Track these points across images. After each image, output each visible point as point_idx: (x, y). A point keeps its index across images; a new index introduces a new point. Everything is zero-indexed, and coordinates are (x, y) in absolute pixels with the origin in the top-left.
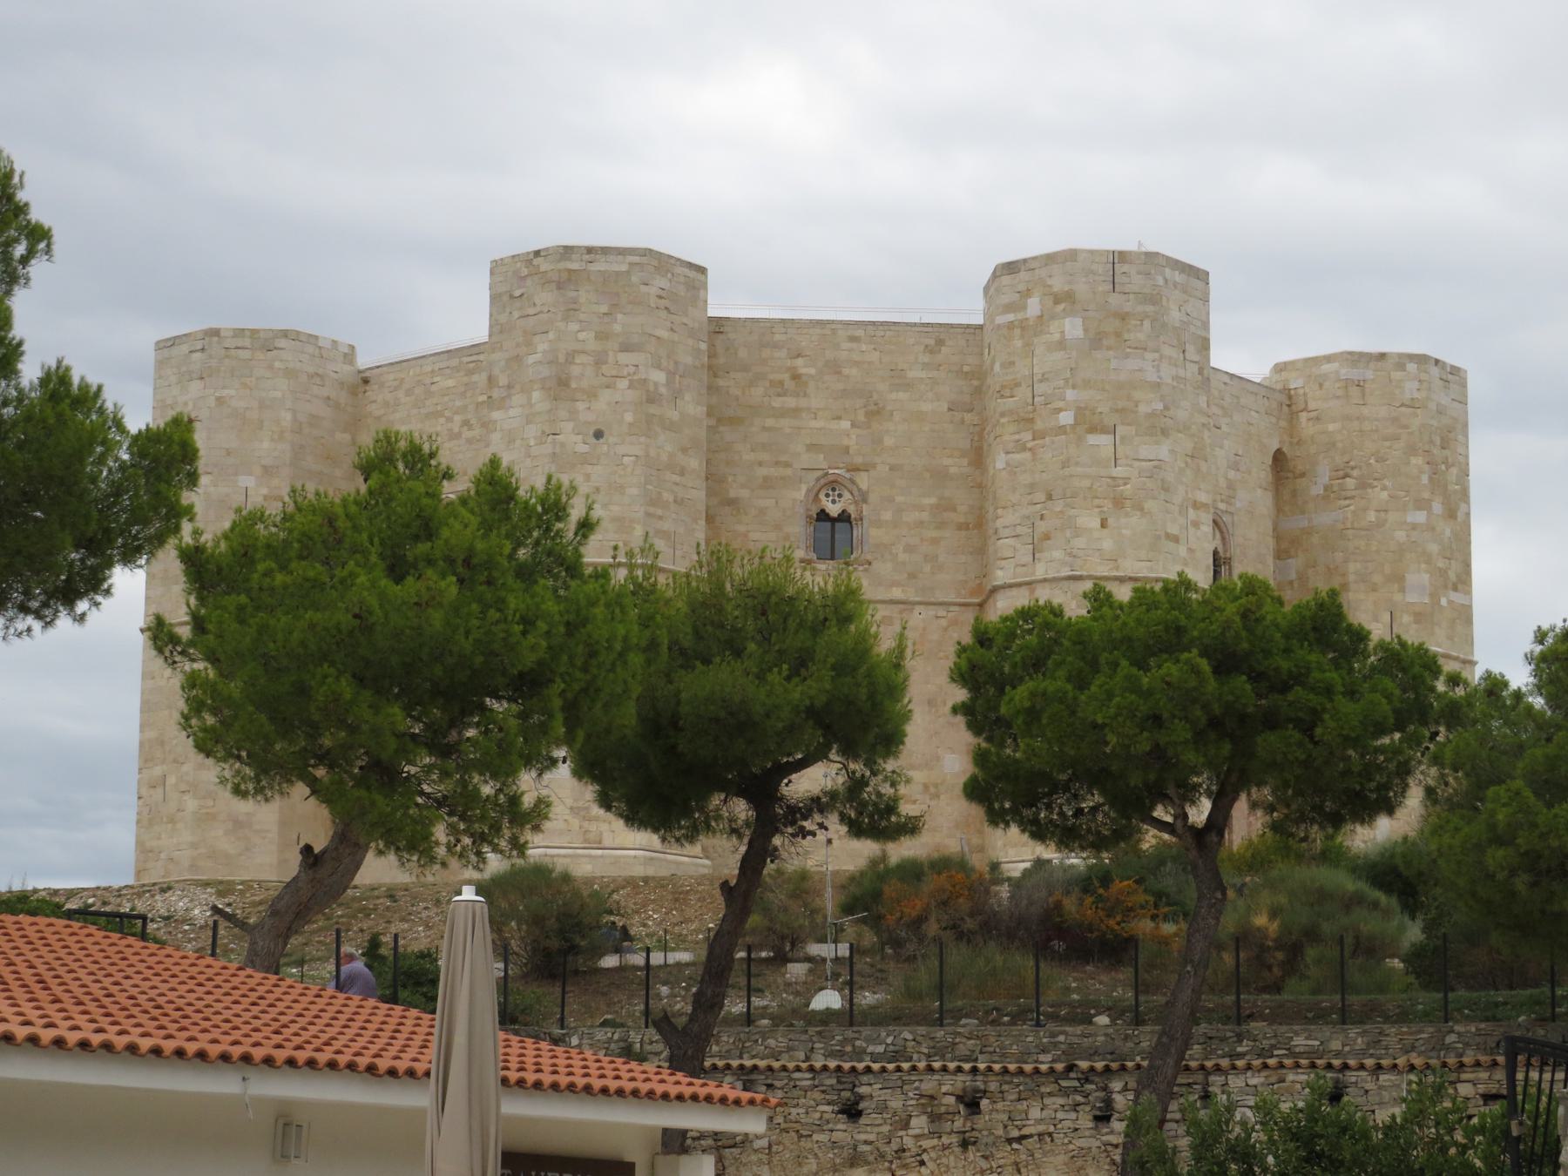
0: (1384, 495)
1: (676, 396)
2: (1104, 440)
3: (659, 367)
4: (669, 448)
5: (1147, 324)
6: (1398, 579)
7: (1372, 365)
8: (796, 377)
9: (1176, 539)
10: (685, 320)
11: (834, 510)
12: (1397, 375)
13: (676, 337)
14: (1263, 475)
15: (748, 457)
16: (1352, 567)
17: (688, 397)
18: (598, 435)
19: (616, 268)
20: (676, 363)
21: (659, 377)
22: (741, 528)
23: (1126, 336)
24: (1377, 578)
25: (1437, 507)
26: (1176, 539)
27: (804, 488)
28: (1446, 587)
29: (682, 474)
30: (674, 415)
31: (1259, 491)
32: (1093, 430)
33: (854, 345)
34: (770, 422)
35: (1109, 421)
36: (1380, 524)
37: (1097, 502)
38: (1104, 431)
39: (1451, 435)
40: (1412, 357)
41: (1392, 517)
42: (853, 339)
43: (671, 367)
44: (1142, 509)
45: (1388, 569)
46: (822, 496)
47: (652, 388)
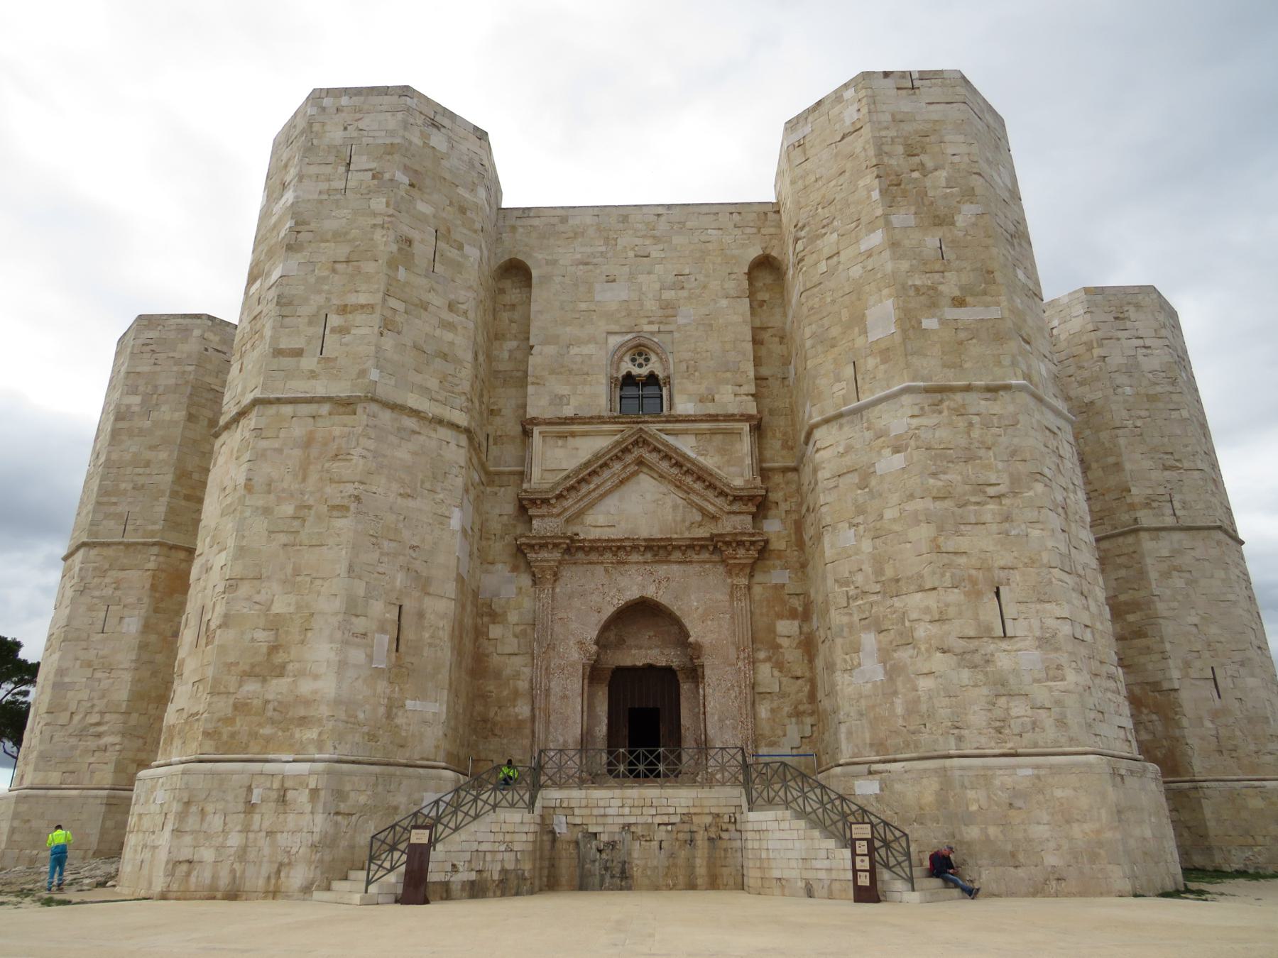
0: (835, 235)
4: (134, 449)
6: (859, 321)
7: (810, 119)
9: (298, 353)
10: (171, 355)
13: (158, 368)
14: (730, 285)
16: (807, 332)
17: (164, 408)
20: (156, 387)
21: (136, 400)
24: (835, 331)
25: (903, 217)
39: (933, 138)
40: (846, 86)
45: (845, 315)
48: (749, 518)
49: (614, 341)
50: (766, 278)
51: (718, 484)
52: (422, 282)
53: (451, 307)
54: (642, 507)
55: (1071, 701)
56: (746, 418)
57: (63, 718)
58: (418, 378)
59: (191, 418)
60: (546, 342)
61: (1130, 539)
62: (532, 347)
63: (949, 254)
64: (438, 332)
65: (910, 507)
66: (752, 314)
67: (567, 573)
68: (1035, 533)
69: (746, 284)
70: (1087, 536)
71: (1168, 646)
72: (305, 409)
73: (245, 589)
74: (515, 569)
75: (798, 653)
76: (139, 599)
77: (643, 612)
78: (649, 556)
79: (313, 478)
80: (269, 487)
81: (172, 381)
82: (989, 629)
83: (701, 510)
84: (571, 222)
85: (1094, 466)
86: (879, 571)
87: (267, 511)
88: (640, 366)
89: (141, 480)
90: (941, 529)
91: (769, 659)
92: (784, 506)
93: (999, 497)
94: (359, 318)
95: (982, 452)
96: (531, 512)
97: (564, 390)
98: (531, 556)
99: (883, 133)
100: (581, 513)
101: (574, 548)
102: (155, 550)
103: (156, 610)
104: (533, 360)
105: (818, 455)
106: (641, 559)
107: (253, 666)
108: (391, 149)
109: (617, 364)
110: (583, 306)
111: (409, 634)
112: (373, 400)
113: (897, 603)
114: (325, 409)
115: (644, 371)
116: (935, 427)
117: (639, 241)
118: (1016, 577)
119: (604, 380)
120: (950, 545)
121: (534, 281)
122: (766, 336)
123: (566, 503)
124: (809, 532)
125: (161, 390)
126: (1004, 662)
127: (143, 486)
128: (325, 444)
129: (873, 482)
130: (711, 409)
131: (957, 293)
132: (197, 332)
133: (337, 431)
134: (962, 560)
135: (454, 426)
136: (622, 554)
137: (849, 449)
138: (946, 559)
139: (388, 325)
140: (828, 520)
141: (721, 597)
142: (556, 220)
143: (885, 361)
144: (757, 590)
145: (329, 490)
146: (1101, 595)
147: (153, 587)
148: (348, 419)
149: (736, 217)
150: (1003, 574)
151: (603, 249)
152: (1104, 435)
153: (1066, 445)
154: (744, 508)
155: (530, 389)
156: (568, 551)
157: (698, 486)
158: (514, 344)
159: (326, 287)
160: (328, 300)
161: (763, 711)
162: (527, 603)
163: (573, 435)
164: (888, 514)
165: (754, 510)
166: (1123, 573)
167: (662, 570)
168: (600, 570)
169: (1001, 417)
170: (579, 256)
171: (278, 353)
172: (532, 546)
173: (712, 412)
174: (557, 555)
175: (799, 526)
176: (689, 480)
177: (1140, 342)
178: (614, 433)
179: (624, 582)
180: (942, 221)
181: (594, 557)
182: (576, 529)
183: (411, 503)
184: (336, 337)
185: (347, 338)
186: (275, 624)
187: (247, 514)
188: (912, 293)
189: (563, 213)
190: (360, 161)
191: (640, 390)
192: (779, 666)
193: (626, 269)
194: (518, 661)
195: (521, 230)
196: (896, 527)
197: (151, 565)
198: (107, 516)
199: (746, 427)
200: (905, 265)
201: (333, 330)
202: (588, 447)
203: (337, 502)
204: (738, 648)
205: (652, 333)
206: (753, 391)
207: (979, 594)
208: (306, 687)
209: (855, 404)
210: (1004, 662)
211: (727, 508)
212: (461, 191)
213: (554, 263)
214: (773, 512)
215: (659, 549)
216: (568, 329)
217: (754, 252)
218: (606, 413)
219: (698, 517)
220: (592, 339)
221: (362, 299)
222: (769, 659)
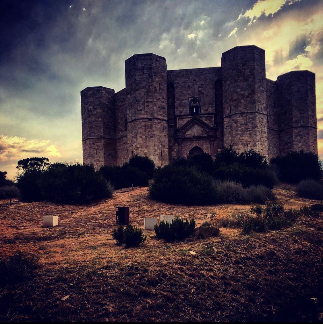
1: (95, 109)
2: (129, 96)
3: (91, 106)
4: (94, 118)
8: (124, 99)
9: (141, 110)
13: (95, 100)
18: (85, 119)
21: (92, 107)
28: (244, 97)
29: (97, 121)
30: (95, 113)
31: (210, 90)
34: (121, 108)
36: (228, 89)
41: (231, 86)
45: (230, 98)
47: (89, 110)
49: (190, 99)
53: (163, 98)
56: (213, 114)
58: (159, 113)
59: (104, 111)
60: (178, 100)
64: (162, 104)
65: (236, 133)
66: (215, 92)
68: (254, 136)
72: (144, 120)
73: (140, 149)
76: (102, 149)
77: (196, 148)
78: (197, 139)
79: (147, 132)
81: (98, 103)
83: (206, 131)
86: (232, 142)
87: (141, 137)
88: (195, 104)
89: (97, 125)
90: (240, 136)
92: (220, 129)
93: (250, 131)
94: (150, 104)
95: (248, 123)
97: (182, 110)
100: (186, 132)
102: (103, 139)
103: (105, 150)
104: (176, 104)
106: (195, 140)
110: (184, 92)
112: (154, 118)
114: (147, 120)
116: (241, 120)
117: (194, 77)
120: (241, 139)
125: (96, 105)
128: (148, 126)
129: (232, 128)
130: (207, 112)
131: (248, 95)
132: (100, 91)
134: (243, 141)
135: (165, 120)
138: (240, 141)
142: (178, 73)
143: (235, 107)
144: (215, 144)
145: (150, 133)
147: (104, 146)
148: (151, 122)
149: (213, 71)
150: (249, 143)
151: (187, 79)
153: (265, 120)
155: (176, 110)
158: (172, 100)
159: (144, 98)
160: (144, 100)
163: (184, 118)
164: (234, 133)
168: (189, 142)
169: (252, 117)
171: (138, 110)
173: (207, 113)
174: (182, 140)
178: (190, 118)
180: (247, 80)
182: (185, 135)
183: (161, 134)
187: (138, 137)
188: (240, 95)
193: (192, 83)
196: (235, 136)
198: (92, 133)
199: (214, 115)
200: (239, 90)
201: (146, 106)
202: (186, 120)
203: (151, 135)
207: (245, 146)
213: (178, 83)
215: (198, 138)
217: (216, 79)
219: (205, 132)
220: (186, 99)
221: (150, 100)
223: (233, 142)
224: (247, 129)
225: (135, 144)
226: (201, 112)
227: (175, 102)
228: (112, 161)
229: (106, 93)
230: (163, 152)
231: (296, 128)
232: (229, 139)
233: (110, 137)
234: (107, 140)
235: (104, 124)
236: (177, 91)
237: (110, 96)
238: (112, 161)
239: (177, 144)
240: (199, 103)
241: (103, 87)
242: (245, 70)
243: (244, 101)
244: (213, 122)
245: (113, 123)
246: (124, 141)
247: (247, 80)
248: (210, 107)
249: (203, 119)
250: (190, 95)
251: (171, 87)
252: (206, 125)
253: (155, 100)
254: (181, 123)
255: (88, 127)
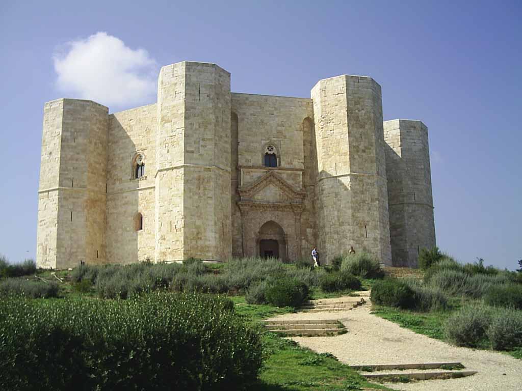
2: (168, 125)
3: (67, 131)
4: (71, 153)
5: (182, 84)
9: (193, 152)
10: (79, 116)
11: (140, 163)
12: (337, 84)
14: (298, 126)
15: (119, 152)
18: (50, 153)
19: (56, 106)
20: (75, 129)
21: (68, 134)
22: (116, 173)
23: (176, 90)
24: (331, 153)
26: (193, 152)
27: (131, 158)
28: (358, 151)
29: (77, 160)
30: (74, 144)
31: (296, 132)
32: (167, 122)
33: (144, 113)
34: (124, 141)
35: (170, 119)
37: (167, 145)
38: (169, 122)
39: (361, 100)
42: (144, 111)
43: (73, 130)
44: (179, 144)
45: (334, 150)
46: (137, 159)
48: (301, 200)
50: (307, 123)
51: (293, 189)
52: (221, 130)
53: (226, 135)
54: (270, 193)
55: (379, 252)
56: (301, 170)
57: (63, 250)
59: (90, 142)
61: (401, 206)
62: (239, 143)
63: (363, 137)
67: (250, 213)
69: (302, 127)
70: (387, 213)
71: (407, 239)
74: (235, 210)
75: (312, 238)
77: (270, 224)
79: (202, 189)
80: (190, 190)
81: (81, 127)
82: (363, 235)
83: (287, 196)
84: (250, 100)
85: (394, 181)
87: (190, 197)
88: (270, 150)
89: (76, 166)
90: (355, 210)
91: (304, 239)
96: (241, 195)
98: (241, 207)
99: (349, 97)
100: (255, 194)
101: (255, 206)
103: (88, 213)
105: (324, 187)
106: (270, 209)
107: (194, 237)
108: (211, 87)
109: (263, 150)
111: (225, 230)
113: (342, 227)
115: (271, 153)
118: (370, 224)
119: (261, 155)
121: (239, 121)
122: (306, 143)
123: (251, 192)
124: (318, 205)
126: (365, 243)
127: (77, 168)
128: (204, 179)
129: (339, 196)
130: (292, 167)
131: (363, 148)
132: (88, 108)
133: (206, 176)
136: (265, 208)
137: (332, 187)
139: (216, 144)
140: (326, 205)
141: (292, 222)
144: (302, 220)
146: (388, 227)
148: (209, 172)
151: (259, 111)
152: (398, 172)
154: (299, 196)
155: (239, 156)
156: (251, 207)
157: (287, 189)
161: (303, 253)
162: (240, 221)
164: (342, 206)
165: (302, 197)
166: (398, 216)
167: (276, 213)
170: (252, 112)
172: (242, 205)
175: (313, 202)
176: (284, 187)
177: (413, 141)
179: (266, 216)
180: (362, 126)
181: (258, 208)
183: (223, 195)
184: (203, 148)
185: (206, 148)
186: (198, 227)
189: (247, 96)
190: (203, 90)
191: (271, 160)
192: (307, 241)
194: (237, 237)
195: (234, 101)
196: (344, 209)
197: (85, 198)
198: (65, 179)
199: (301, 173)
200: (352, 139)
204: (296, 235)
205: (275, 141)
206: (303, 162)
208: (207, 243)
209: (336, 175)
210: (365, 243)
211: (295, 196)
212: (226, 97)
213: (244, 114)
214: (306, 198)
215: (275, 207)
216: (249, 137)
217: (305, 116)
218: (261, 166)
221: (209, 137)
222: (304, 239)
223: (341, 220)
224: (364, 202)
225: (178, 209)
226: (280, 165)
227: (238, 143)
228: (98, 235)
229: (96, 111)
230: (224, 226)
231: (409, 204)
232: (334, 214)
233: (96, 189)
234: (92, 194)
235: (90, 165)
236: (241, 125)
237: (101, 119)
238: (98, 235)
239: (238, 214)
240: (278, 150)
241: (92, 102)
242: (359, 111)
243: (359, 156)
244: (299, 182)
245: (102, 165)
246: (126, 200)
247: (362, 126)
248: (296, 158)
249: (284, 176)
250: (264, 136)
251: (235, 117)
252: (288, 187)
253: (216, 138)
254: (246, 178)
255: (57, 168)
